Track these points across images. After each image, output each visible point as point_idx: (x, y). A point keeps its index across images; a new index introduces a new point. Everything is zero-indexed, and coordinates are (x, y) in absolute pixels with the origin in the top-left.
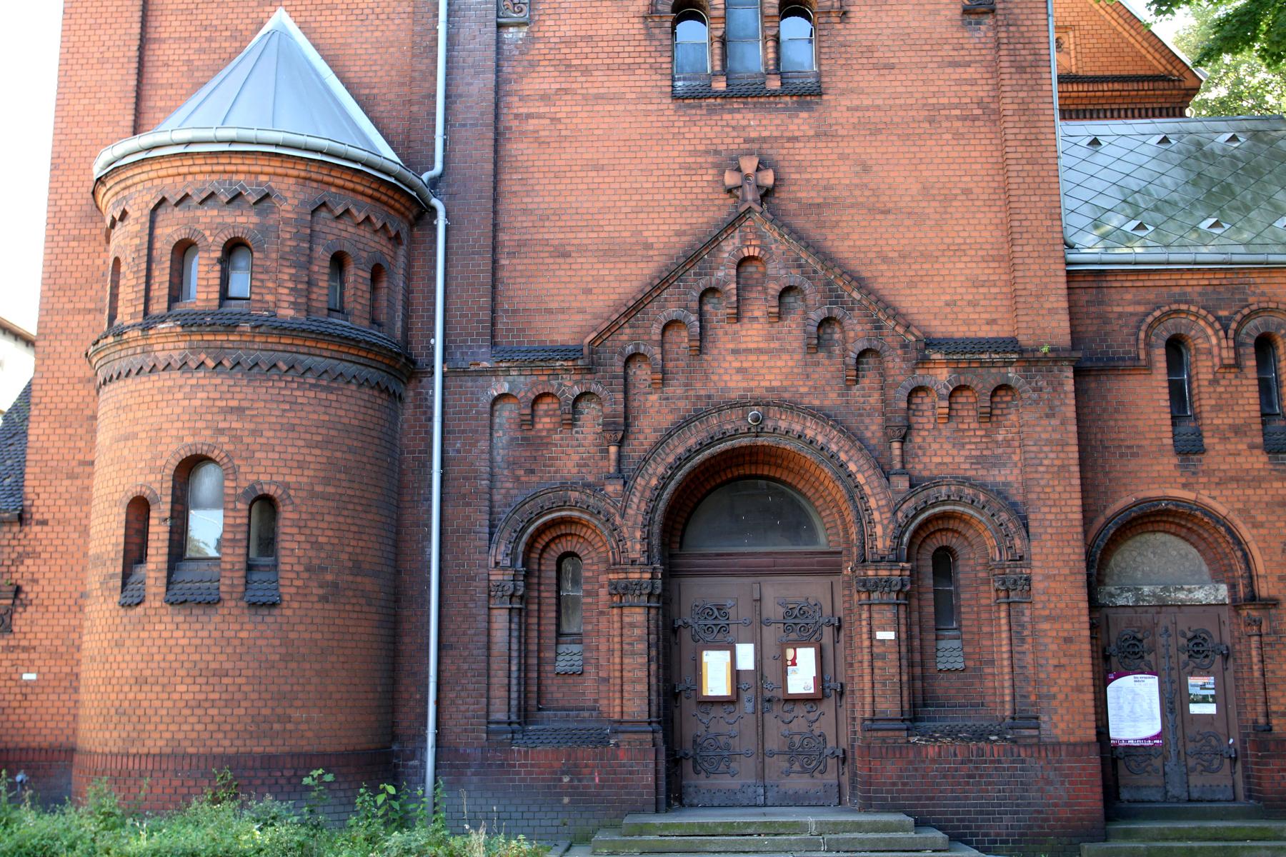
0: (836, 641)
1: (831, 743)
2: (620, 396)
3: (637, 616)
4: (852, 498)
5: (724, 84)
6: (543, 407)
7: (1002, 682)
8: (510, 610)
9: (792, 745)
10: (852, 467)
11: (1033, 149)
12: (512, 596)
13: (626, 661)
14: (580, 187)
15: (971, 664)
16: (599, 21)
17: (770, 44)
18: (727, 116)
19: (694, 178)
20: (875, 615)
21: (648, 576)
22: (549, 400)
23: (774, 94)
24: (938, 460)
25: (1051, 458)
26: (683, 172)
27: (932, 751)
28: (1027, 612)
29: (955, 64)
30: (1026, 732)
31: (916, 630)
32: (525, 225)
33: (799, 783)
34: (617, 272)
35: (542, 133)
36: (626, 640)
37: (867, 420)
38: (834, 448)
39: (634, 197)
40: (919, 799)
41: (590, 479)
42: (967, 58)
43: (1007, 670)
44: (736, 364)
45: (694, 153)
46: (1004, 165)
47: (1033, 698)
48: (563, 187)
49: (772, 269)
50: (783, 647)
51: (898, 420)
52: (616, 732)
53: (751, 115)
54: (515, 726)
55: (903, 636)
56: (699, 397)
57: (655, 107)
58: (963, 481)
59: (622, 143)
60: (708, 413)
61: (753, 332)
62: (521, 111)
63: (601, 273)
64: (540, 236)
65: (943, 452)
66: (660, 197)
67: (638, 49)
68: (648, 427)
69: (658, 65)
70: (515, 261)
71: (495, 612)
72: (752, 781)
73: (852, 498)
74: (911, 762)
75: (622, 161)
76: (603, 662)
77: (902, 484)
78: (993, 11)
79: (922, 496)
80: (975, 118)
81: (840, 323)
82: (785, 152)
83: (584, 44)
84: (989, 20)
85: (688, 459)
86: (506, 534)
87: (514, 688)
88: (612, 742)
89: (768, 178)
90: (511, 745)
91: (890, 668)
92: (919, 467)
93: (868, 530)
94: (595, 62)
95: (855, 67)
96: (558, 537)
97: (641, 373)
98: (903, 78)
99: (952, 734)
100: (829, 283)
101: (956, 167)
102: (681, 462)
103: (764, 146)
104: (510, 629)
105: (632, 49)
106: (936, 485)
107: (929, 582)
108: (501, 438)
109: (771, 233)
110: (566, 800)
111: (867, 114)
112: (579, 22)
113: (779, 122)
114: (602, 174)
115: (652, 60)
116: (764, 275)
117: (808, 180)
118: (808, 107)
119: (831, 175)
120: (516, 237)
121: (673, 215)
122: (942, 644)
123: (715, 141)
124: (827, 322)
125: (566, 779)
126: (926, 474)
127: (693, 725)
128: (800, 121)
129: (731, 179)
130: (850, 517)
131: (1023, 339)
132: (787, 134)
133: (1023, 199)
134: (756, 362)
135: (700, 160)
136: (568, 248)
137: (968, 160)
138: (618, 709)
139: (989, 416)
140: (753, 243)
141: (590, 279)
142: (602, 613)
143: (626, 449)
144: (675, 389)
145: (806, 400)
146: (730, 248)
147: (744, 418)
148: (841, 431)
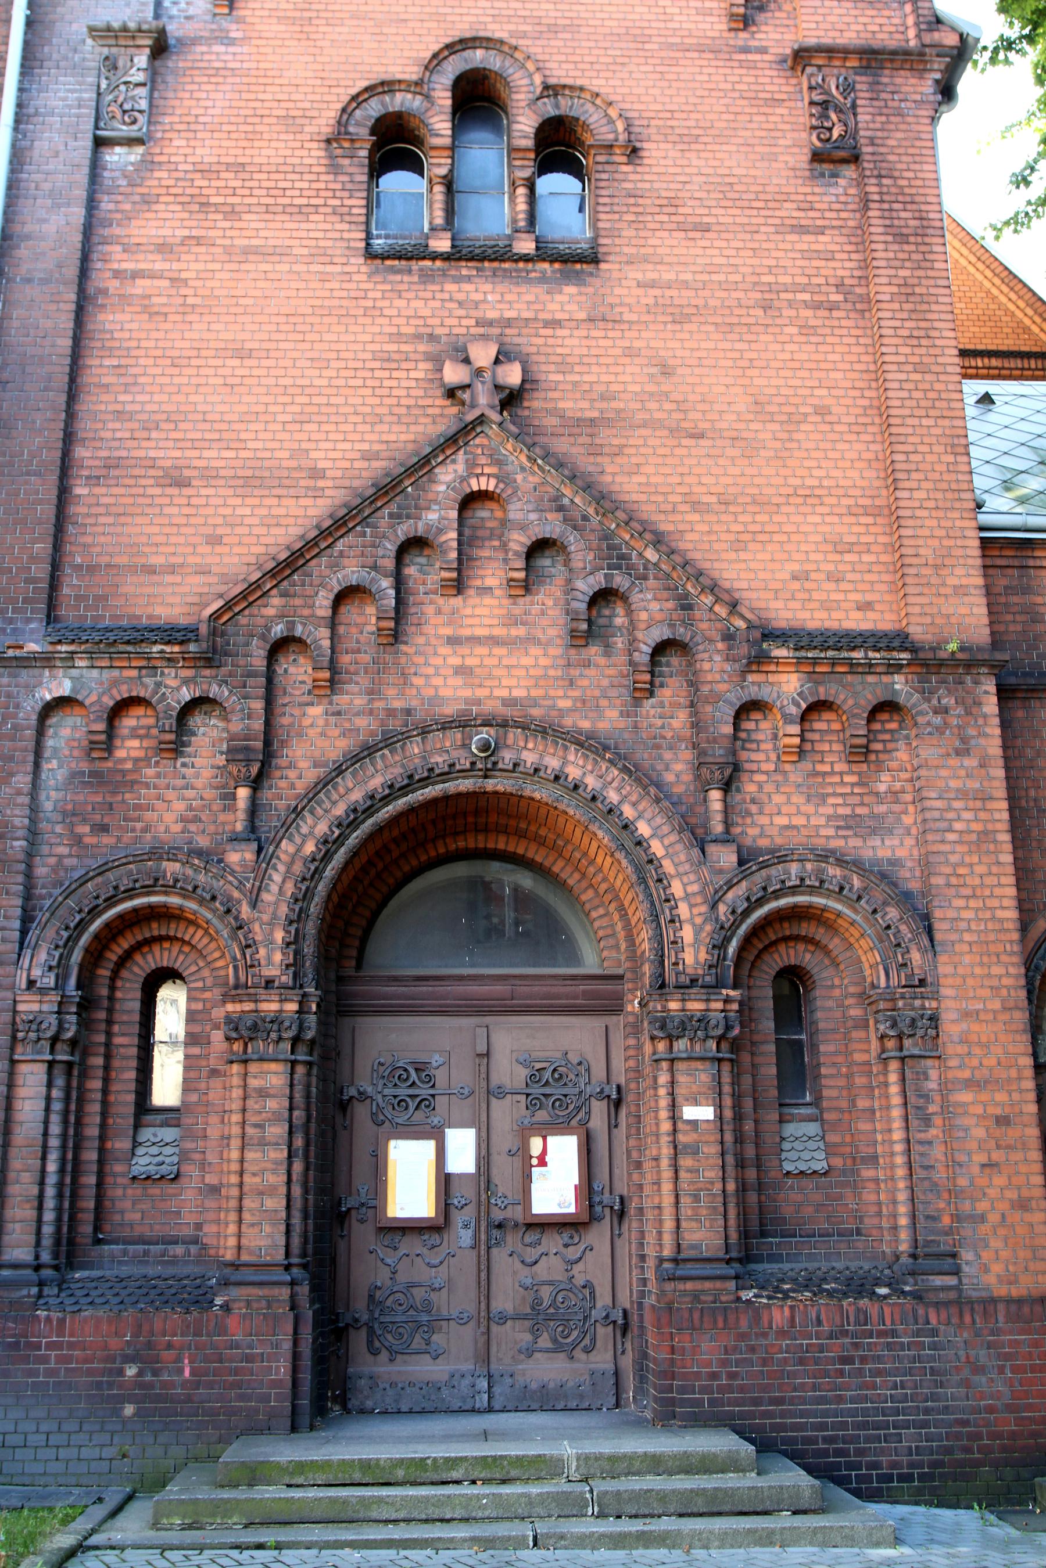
0: (613, 1126)
1: (603, 1299)
2: (258, 705)
3: (272, 1077)
4: (643, 880)
5: (448, 243)
6: (128, 722)
7: (894, 1191)
8: (51, 1064)
9: (537, 1302)
10: (643, 829)
11: (923, 351)
12: (55, 1040)
13: (249, 1155)
14: (211, 381)
15: (837, 1162)
16: (256, 144)
17: (521, 191)
18: (450, 287)
19: (395, 374)
20: (681, 1078)
21: (293, 1007)
22: (140, 711)
23: (526, 258)
24: (782, 821)
25: (965, 820)
26: (378, 364)
27: (779, 1316)
28: (933, 1074)
29: (802, 230)
30: (938, 1281)
31: (748, 1103)
32: (118, 435)
33: (547, 1369)
34: (264, 512)
35: (155, 300)
36: (251, 1118)
37: (668, 755)
38: (613, 797)
39: (299, 400)
40: (756, 1402)
41: (203, 842)
42: (819, 223)
43: (901, 1172)
44: (455, 661)
45: (398, 337)
46: (878, 375)
47: (946, 1220)
48: (185, 380)
49: (516, 511)
50: (524, 1134)
51: (719, 753)
52: (226, 1283)
53: (488, 287)
54: (47, 1273)
55: (728, 1114)
56: (391, 712)
57: (338, 269)
58: (824, 856)
59: (283, 319)
60: (405, 737)
61: (484, 609)
62: (125, 266)
63: (239, 511)
64: (142, 453)
65: (792, 807)
66: (340, 400)
67: (314, 185)
68: (303, 759)
69: (345, 210)
70: (97, 490)
71: (23, 1068)
72: (467, 1367)
73: (643, 880)
74: (742, 1337)
75: (282, 345)
76: (212, 1158)
77: (726, 857)
78: (855, 159)
79: (759, 878)
80: (832, 307)
81: (624, 598)
82: (540, 341)
83: (232, 175)
84: (849, 172)
85: (369, 811)
86: (50, 933)
87: (50, 1203)
88: (218, 1301)
89: (512, 375)
90: (35, 1306)
91: (706, 1169)
92: (753, 832)
93: (668, 934)
94: (247, 200)
95: (650, 226)
96: (149, 942)
97: (297, 671)
98: (724, 244)
99: (812, 1283)
100: (607, 536)
101: (806, 374)
102: (356, 816)
103: (508, 331)
104: (48, 1099)
105: (306, 185)
106: (782, 860)
107: (768, 1025)
108: (55, 771)
109: (515, 457)
110: (129, 1410)
111: (668, 293)
112: (225, 143)
113: (530, 298)
114: (247, 362)
115: (338, 202)
116: (504, 522)
117: (575, 384)
118: (578, 279)
119: (612, 378)
120: (104, 454)
121: (360, 428)
122: (790, 1129)
123: (430, 322)
124: (603, 597)
125: (131, 1371)
126: (764, 843)
127: (370, 1268)
128: (565, 298)
129: (454, 374)
130: (639, 913)
131: (917, 632)
132: (542, 316)
133: (910, 421)
134: (486, 657)
135: (404, 348)
136: (187, 473)
137: (823, 366)
138: (232, 1242)
139: (862, 753)
140: (487, 470)
141: (220, 521)
142: (214, 1073)
143: (266, 795)
144: (352, 697)
145: (568, 722)
146: (449, 477)
147: (465, 746)
148: (625, 770)
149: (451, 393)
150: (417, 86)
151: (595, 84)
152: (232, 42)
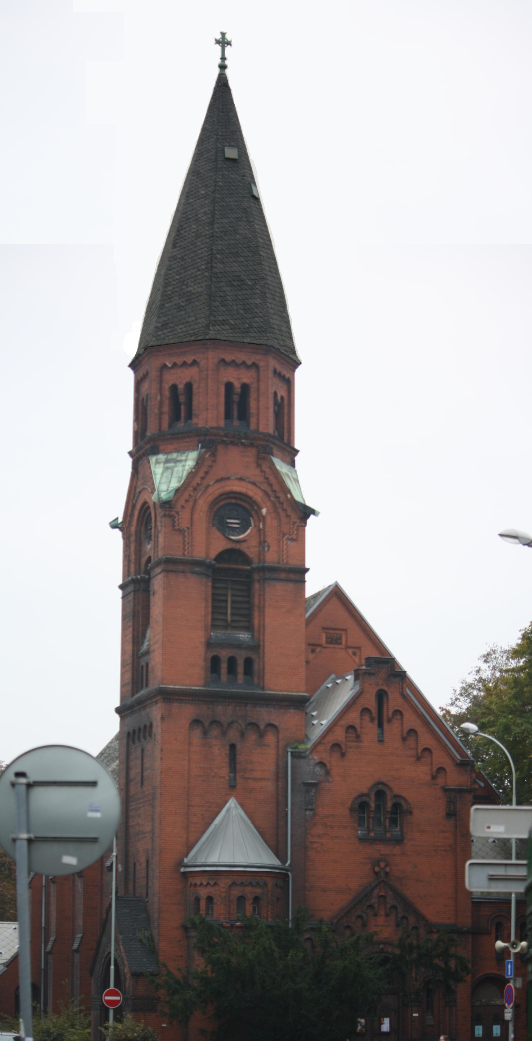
62: (312, 840)
78: (455, 815)
89: (388, 869)
124: (404, 917)
129: (377, 869)
146: (376, 892)
149: (376, 874)
150: (367, 795)
151: (404, 794)
152: (330, 782)
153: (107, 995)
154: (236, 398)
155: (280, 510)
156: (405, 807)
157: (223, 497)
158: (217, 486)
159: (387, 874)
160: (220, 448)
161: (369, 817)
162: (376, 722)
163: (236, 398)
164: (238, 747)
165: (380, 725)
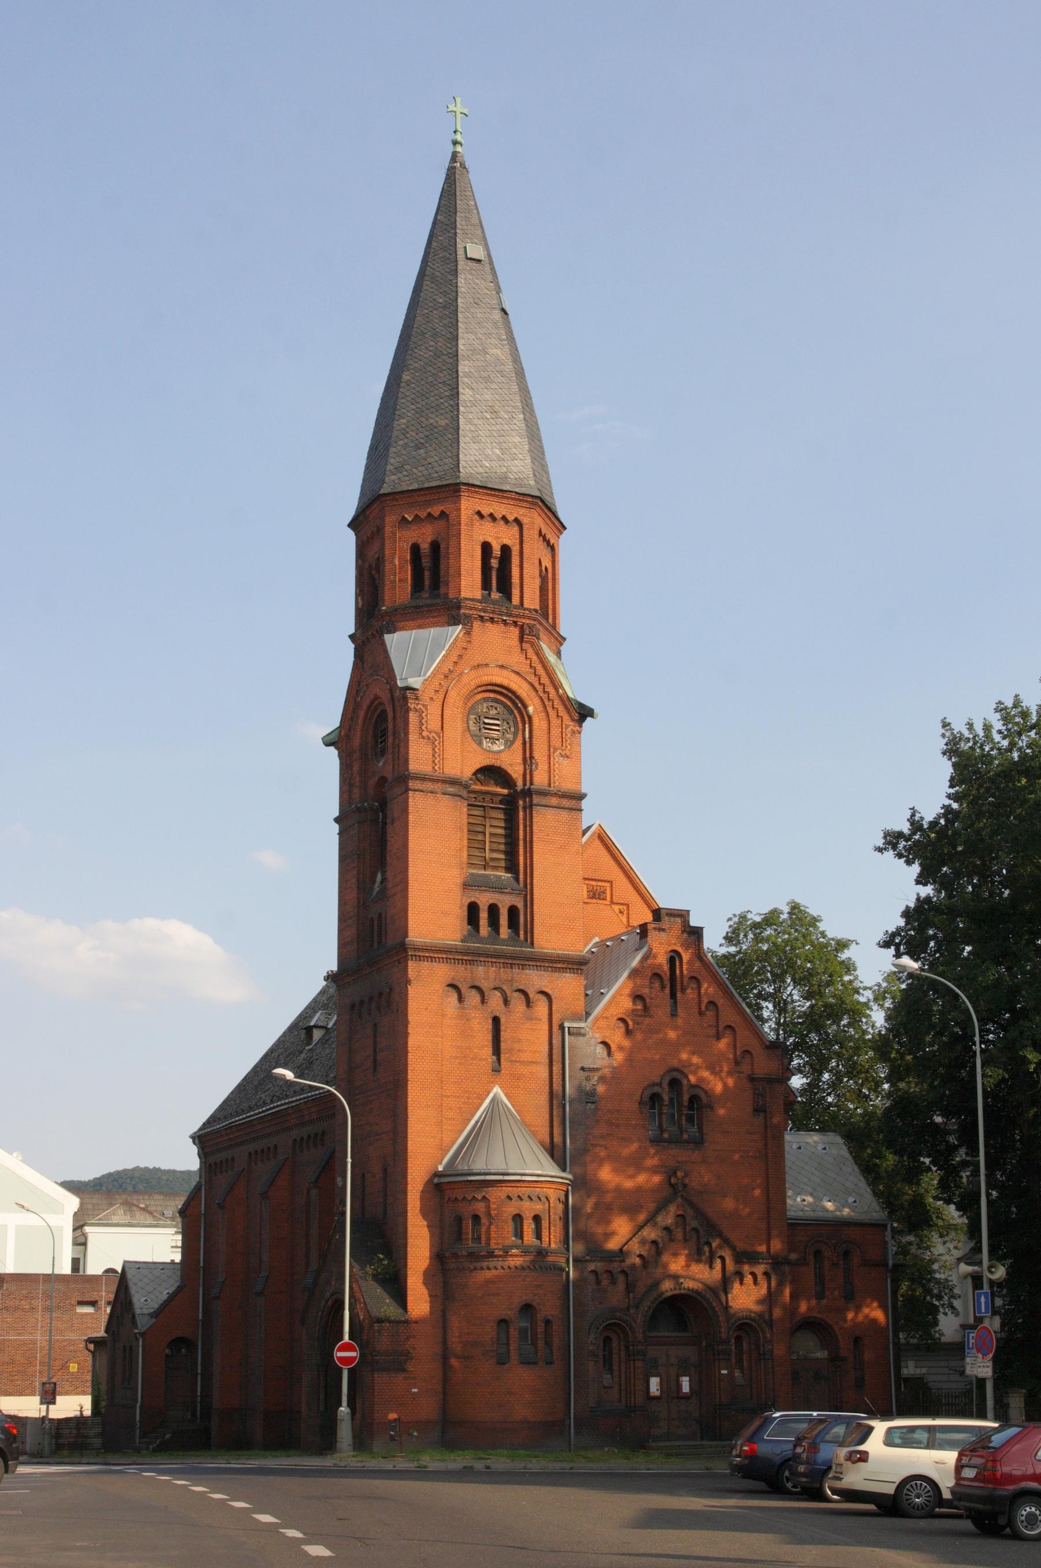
78: (765, 1111)
84: (762, 1115)
129: (673, 1180)
150: (660, 1085)
153: (340, 1350)
154: (494, 563)
155: (550, 710)
156: (705, 1100)
157: (480, 689)
158: (474, 673)
159: (685, 1186)
160: (477, 624)
161: (660, 1114)
162: (667, 991)
163: (494, 563)
164: (503, 1020)
165: (673, 995)
